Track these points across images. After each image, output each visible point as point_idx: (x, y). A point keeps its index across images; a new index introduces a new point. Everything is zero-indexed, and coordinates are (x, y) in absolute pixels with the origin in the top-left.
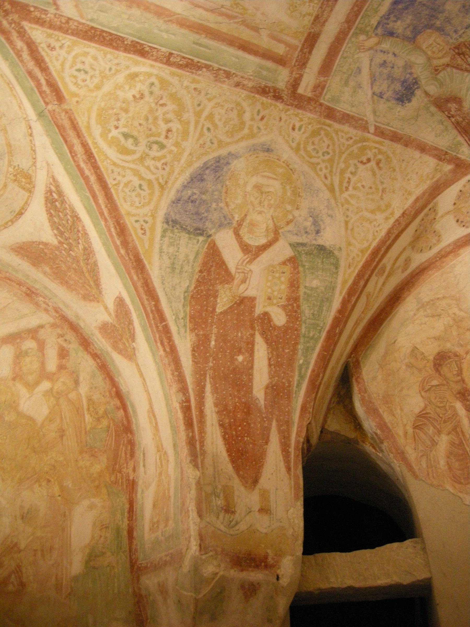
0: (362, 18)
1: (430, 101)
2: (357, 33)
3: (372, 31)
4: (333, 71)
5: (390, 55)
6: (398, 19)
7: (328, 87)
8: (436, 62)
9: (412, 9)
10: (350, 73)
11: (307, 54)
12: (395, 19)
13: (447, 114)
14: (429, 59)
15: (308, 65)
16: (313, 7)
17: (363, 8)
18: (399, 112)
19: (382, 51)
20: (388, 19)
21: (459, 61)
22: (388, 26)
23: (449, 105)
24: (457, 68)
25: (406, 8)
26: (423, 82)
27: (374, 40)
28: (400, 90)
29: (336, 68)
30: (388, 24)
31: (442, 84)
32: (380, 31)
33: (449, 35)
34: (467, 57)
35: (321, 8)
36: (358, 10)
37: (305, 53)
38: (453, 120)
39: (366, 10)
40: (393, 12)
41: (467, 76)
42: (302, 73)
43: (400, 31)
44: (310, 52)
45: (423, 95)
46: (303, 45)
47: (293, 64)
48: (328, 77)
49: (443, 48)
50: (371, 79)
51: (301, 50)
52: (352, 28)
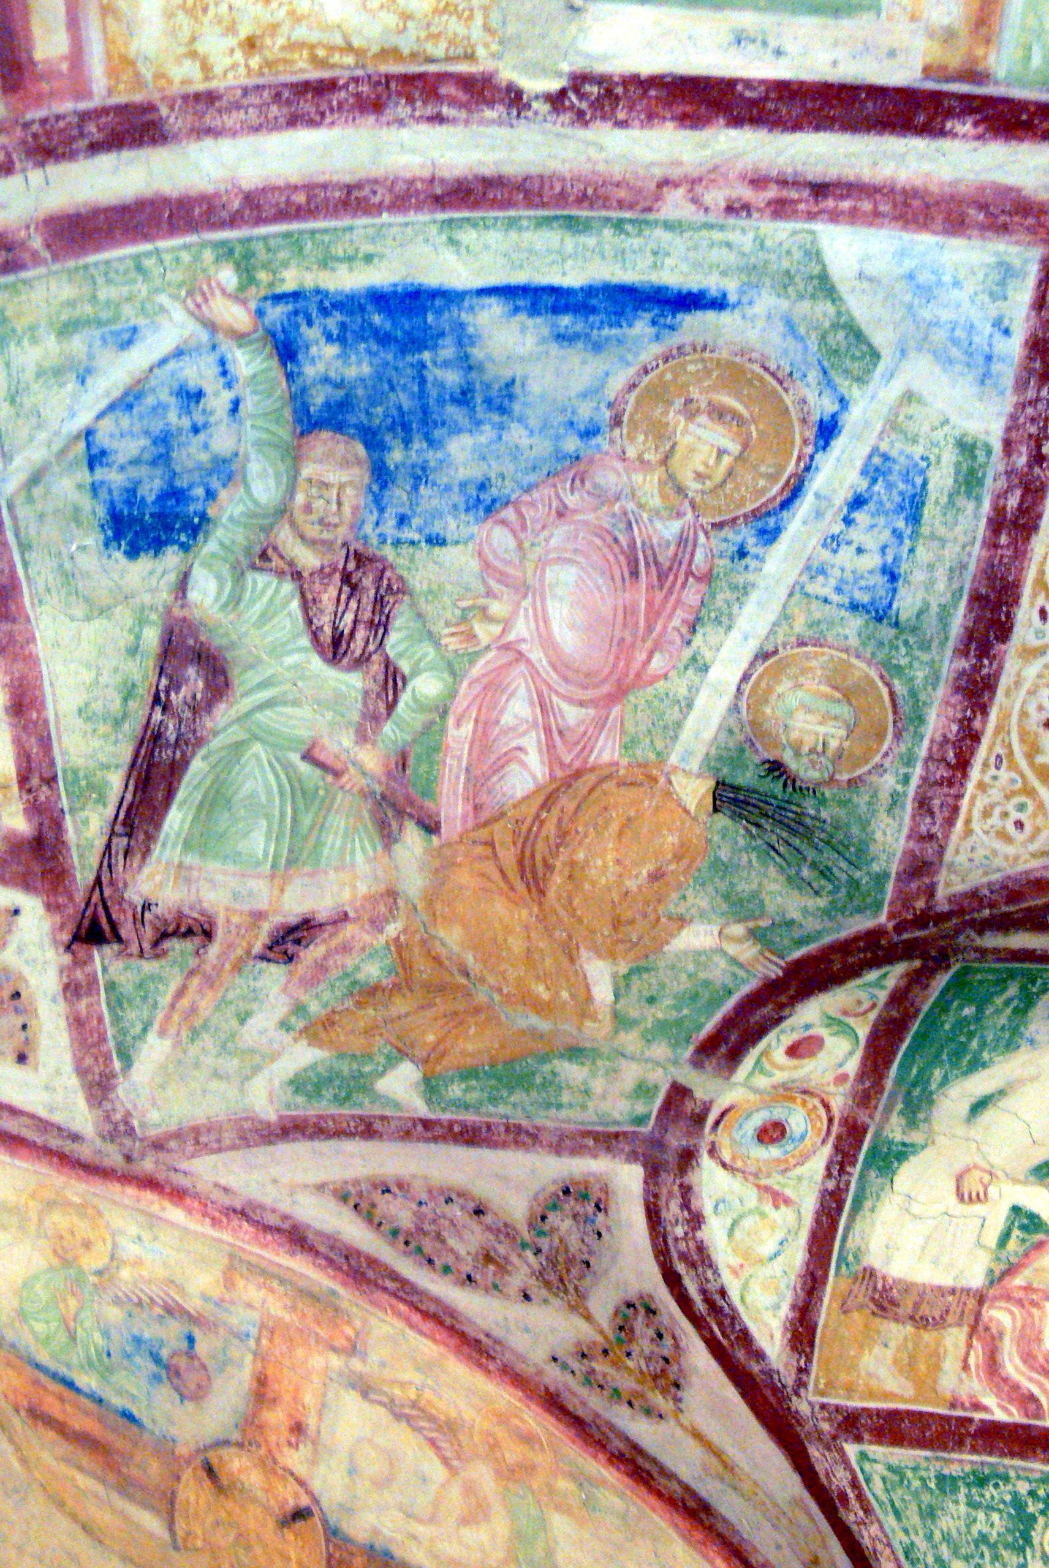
0: (287, 235)
1: (169, 611)
2: (231, 252)
3: (263, 293)
4: (81, 262)
5: (227, 396)
6: (341, 338)
7: (25, 282)
8: (285, 536)
9: (390, 357)
10: (104, 315)
11: (83, 143)
12: (335, 332)
13: (162, 687)
14: (283, 511)
15: (54, 170)
16: (234, 66)
17: (315, 218)
18: (82, 548)
19: (222, 362)
20: (325, 312)
21: (328, 596)
22: (304, 328)
23: (191, 671)
24: (305, 606)
25: (384, 339)
26: (210, 546)
27: (238, 316)
28: (143, 499)
29: (96, 264)
30: (310, 323)
31: (235, 600)
32: (276, 313)
33: (382, 510)
34: (353, 605)
35: (245, 91)
36: (299, 208)
37: (82, 135)
38: (158, 716)
39: (313, 232)
40: (351, 313)
41: (300, 650)
42: (18, 165)
43: (309, 373)
44: (95, 148)
45: (172, 577)
46: (104, 111)
47: (29, 116)
48: (56, 258)
49: (336, 526)
50: (126, 394)
51: (85, 117)
52: (239, 227)
